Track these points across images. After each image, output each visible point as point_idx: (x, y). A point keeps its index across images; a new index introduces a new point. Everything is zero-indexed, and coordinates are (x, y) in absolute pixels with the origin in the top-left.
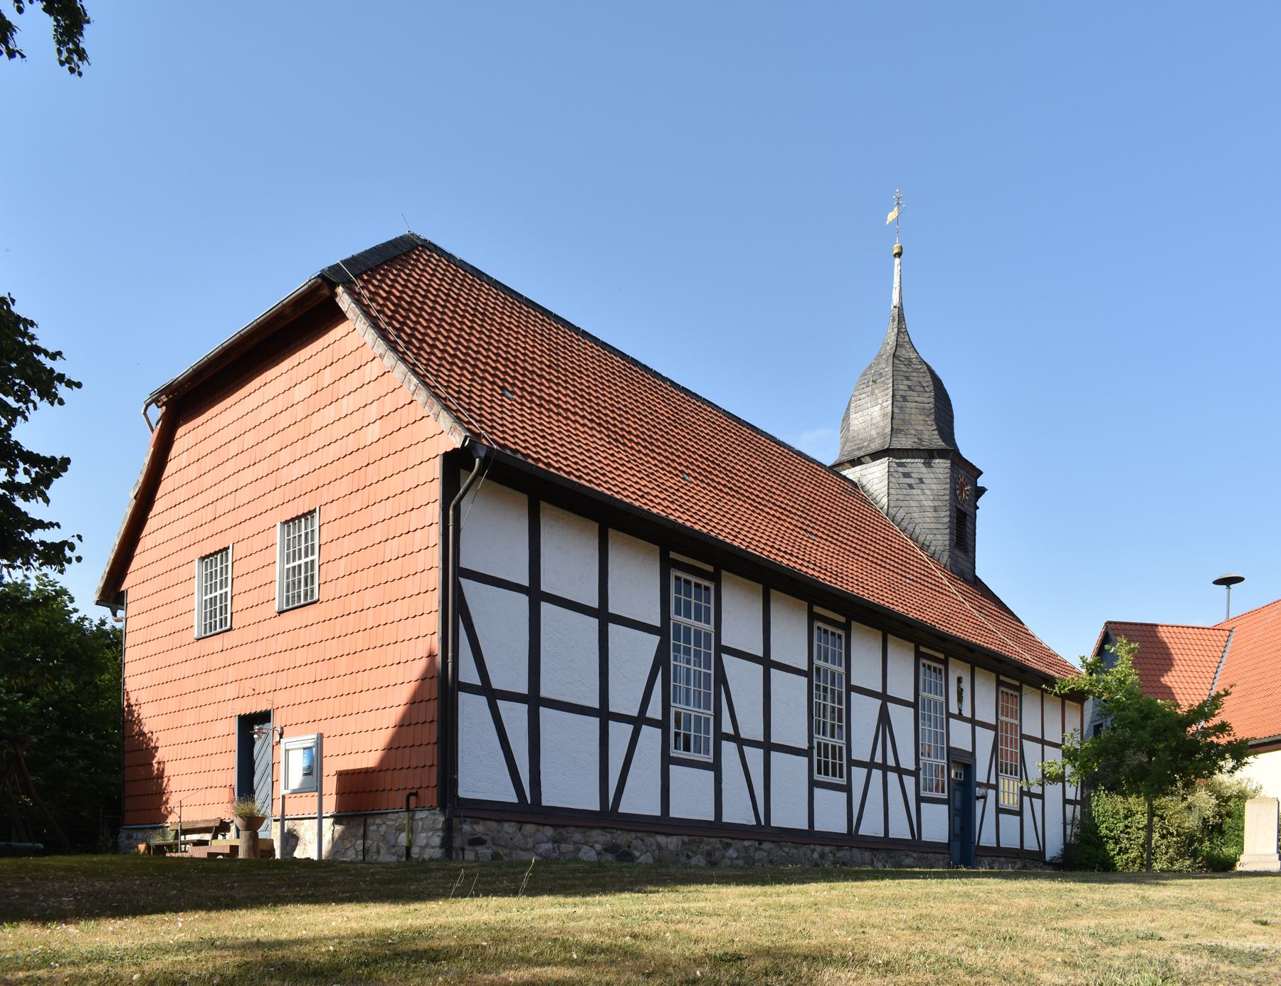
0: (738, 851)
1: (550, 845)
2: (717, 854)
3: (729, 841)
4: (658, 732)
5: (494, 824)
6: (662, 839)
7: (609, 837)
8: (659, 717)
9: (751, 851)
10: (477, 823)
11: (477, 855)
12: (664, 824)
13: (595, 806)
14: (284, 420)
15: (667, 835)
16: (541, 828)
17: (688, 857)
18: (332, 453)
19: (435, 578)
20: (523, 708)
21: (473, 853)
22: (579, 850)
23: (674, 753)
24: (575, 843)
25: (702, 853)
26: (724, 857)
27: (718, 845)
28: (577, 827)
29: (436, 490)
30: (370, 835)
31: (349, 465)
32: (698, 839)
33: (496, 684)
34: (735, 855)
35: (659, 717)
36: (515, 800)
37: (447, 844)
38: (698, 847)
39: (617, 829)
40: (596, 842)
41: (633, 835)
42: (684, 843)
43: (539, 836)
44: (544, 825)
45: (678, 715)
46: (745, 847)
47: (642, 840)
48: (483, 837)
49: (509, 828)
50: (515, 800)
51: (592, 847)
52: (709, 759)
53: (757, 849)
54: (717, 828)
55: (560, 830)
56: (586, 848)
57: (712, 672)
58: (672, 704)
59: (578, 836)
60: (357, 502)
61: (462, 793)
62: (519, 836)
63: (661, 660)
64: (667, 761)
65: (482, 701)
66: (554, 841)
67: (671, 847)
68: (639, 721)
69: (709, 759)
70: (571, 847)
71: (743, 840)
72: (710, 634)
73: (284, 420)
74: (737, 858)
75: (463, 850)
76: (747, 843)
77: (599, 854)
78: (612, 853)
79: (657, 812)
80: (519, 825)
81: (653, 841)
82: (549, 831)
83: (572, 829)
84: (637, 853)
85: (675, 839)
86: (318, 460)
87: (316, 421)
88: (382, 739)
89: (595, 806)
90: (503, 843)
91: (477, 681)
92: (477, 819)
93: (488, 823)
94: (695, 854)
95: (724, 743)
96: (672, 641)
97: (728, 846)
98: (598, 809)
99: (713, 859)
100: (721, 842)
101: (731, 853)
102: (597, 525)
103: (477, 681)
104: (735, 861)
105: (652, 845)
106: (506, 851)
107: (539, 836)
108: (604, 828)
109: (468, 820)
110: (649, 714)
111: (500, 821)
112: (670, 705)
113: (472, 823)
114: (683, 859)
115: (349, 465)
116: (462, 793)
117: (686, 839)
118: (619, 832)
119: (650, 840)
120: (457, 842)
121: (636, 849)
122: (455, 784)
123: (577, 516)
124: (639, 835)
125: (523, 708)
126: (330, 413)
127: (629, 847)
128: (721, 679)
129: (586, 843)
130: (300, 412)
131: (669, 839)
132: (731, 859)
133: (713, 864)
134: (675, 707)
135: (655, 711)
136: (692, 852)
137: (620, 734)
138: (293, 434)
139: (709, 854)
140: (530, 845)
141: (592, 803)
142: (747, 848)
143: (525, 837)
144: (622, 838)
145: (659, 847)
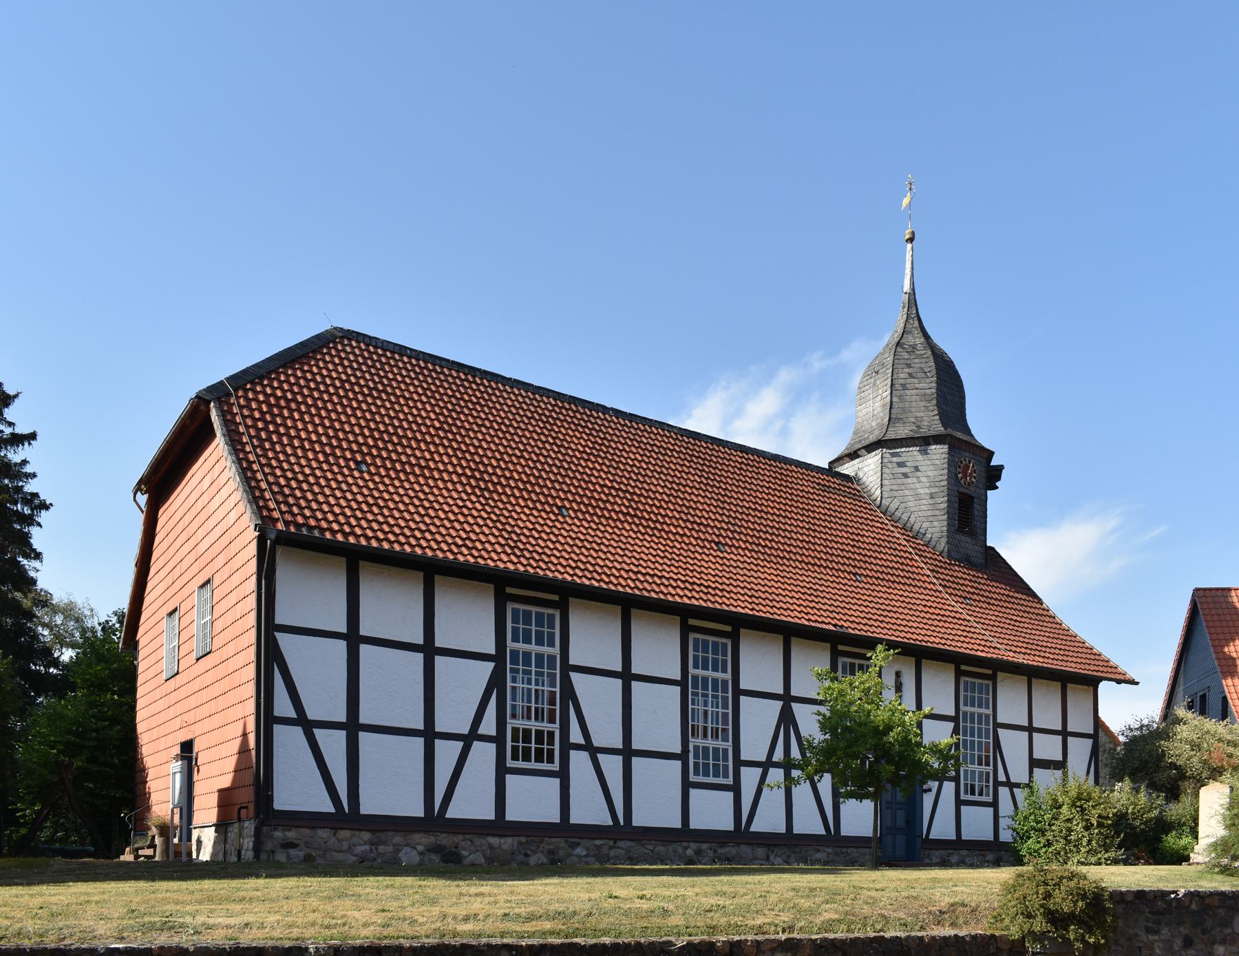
0: (588, 849)
1: (367, 847)
2: (561, 852)
3: (576, 840)
4: (492, 748)
5: (306, 831)
6: (494, 841)
7: (432, 839)
8: (494, 733)
9: (605, 850)
10: (290, 830)
11: (288, 857)
12: (500, 825)
13: (419, 812)
15: (501, 836)
16: (357, 833)
17: (526, 855)
20: (341, 735)
21: (285, 855)
22: (398, 851)
23: (510, 763)
24: (394, 845)
25: (542, 852)
26: (569, 855)
27: (563, 844)
28: (396, 831)
30: (229, 841)
32: (537, 839)
33: (312, 714)
34: (585, 853)
35: (494, 733)
36: (333, 810)
37: (257, 849)
38: (538, 846)
39: (441, 832)
40: (419, 844)
41: (461, 837)
42: (520, 843)
43: (355, 840)
44: (360, 830)
45: (515, 730)
46: (596, 846)
47: (472, 841)
48: (295, 841)
49: (323, 833)
50: (333, 810)
51: (415, 848)
52: (556, 767)
53: (611, 848)
54: (565, 829)
55: (380, 834)
56: (407, 849)
57: (558, 690)
58: (508, 721)
59: (398, 839)
61: (278, 805)
62: (333, 840)
63: (496, 683)
64: (502, 771)
65: (298, 731)
66: (372, 843)
67: (505, 847)
68: (469, 739)
69: (556, 767)
70: (390, 849)
71: (595, 839)
72: (555, 657)
74: (586, 856)
75: (273, 852)
76: (598, 842)
77: (421, 854)
78: (437, 853)
79: (490, 815)
80: (333, 831)
81: (483, 842)
82: (366, 836)
83: (392, 833)
84: (465, 853)
85: (509, 840)
88: (231, 764)
89: (419, 812)
90: (316, 846)
91: (293, 714)
92: (288, 827)
93: (300, 830)
94: (535, 852)
95: (573, 753)
96: (508, 666)
97: (574, 846)
98: (422, 815)
99: (556, 857)
100: (566, 842)
101: (579, 851)
102: (421, 574)
103: (293, 714)
104: (583, 859)
105: (482, 846)
106: (318, 852)
107: (355, 840)
108: (427, 832)
109: (280, 828)
110: (481, 731)
111: (313, 828)
112: (506, 722)
113: (284, 830)
114: (520, 858)
116: (278, 805)
117: (523, 839)
118: (444, 835)
119: (479, 841)
120: (269, 846)
121: (464, 849)
122: (270, 799)
123: (398, 569)
124: (467, 837)
125: (341, 735)
127: (456, 847)
128: (569, 693)
129: (407, 845)
131: (503, 840)
132: (579, 857)
133: (553, 862)
134: (511, 723)
135: (489, 726)
136: (532, 851)
137: (447, 753)
139: (551, 852)
140: (345, 847)
141: (416, 809)
142: (599, 847)
143: (340, 841)
144: (446, 840)
145: (491, 847)
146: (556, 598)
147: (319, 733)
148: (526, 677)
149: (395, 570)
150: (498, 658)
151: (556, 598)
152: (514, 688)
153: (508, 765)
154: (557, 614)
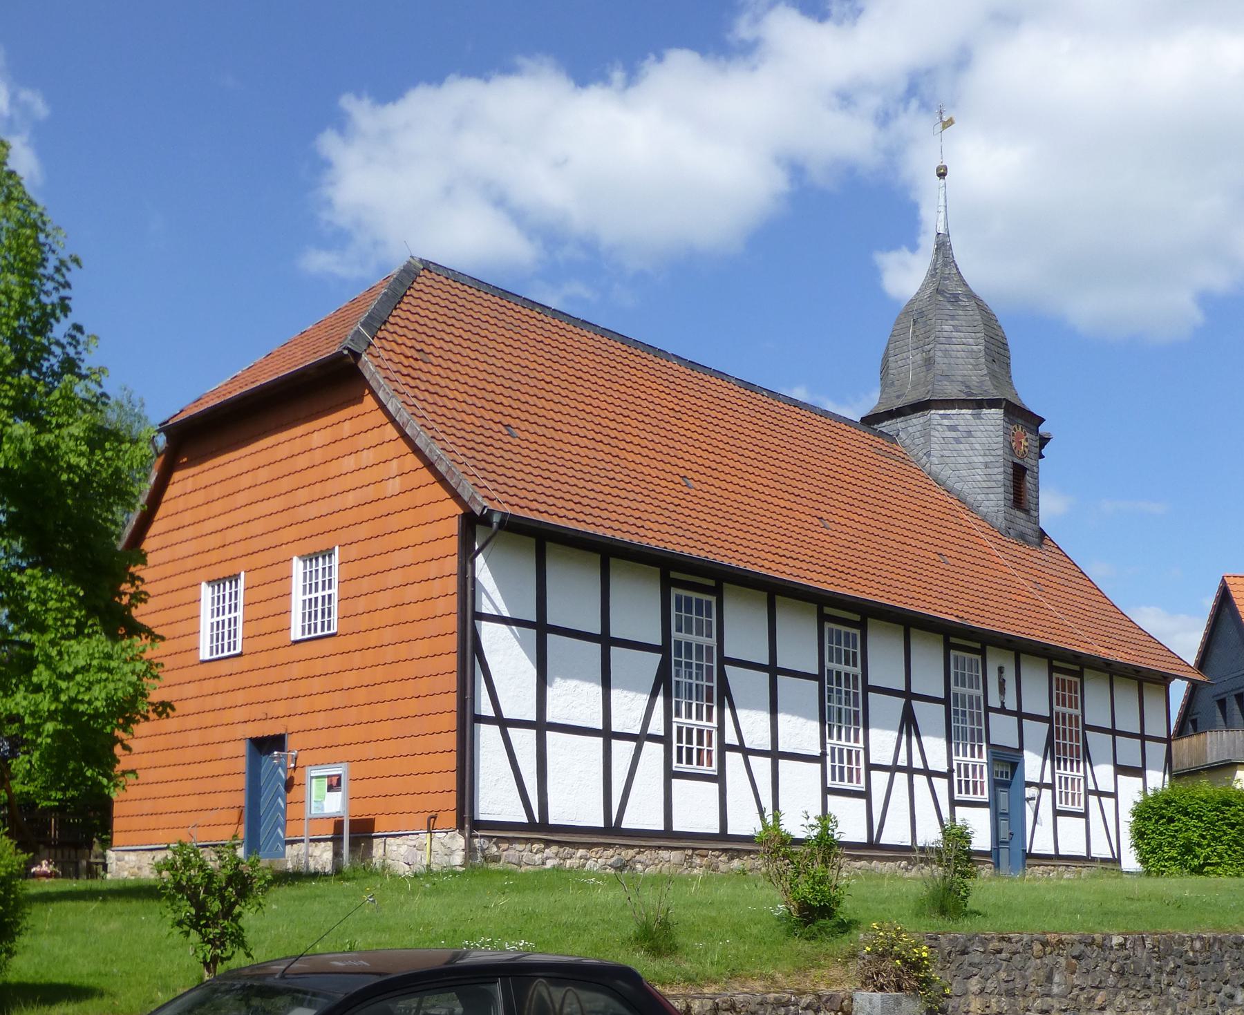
12: (668, 836)
14: (302, 462)
18: (351, 499)
19: (452, 623)
20: (532, 733)
29: (453, 545)
31: (368, 511)
52: (713, 769)
60: (375, 546)
64: (670, 775)
65: (495, 730)
73: (302, 462)
86: (337, 503)
87: (334, 468)
96: (673, 658)
110: (650, 731)
115: (368, 511)
125: (532, 733)
126: (349, 463)
130: (318, 456)
135: (657, 727)
138: (311, 476)
146: (711, 583)
147: (512, 732)
148: (688, 670)
149: (577, 552)
150: (664, 649)
151: (711, 583)
152: (678, 682)
153: (674, 769)
154: (713, 599)
